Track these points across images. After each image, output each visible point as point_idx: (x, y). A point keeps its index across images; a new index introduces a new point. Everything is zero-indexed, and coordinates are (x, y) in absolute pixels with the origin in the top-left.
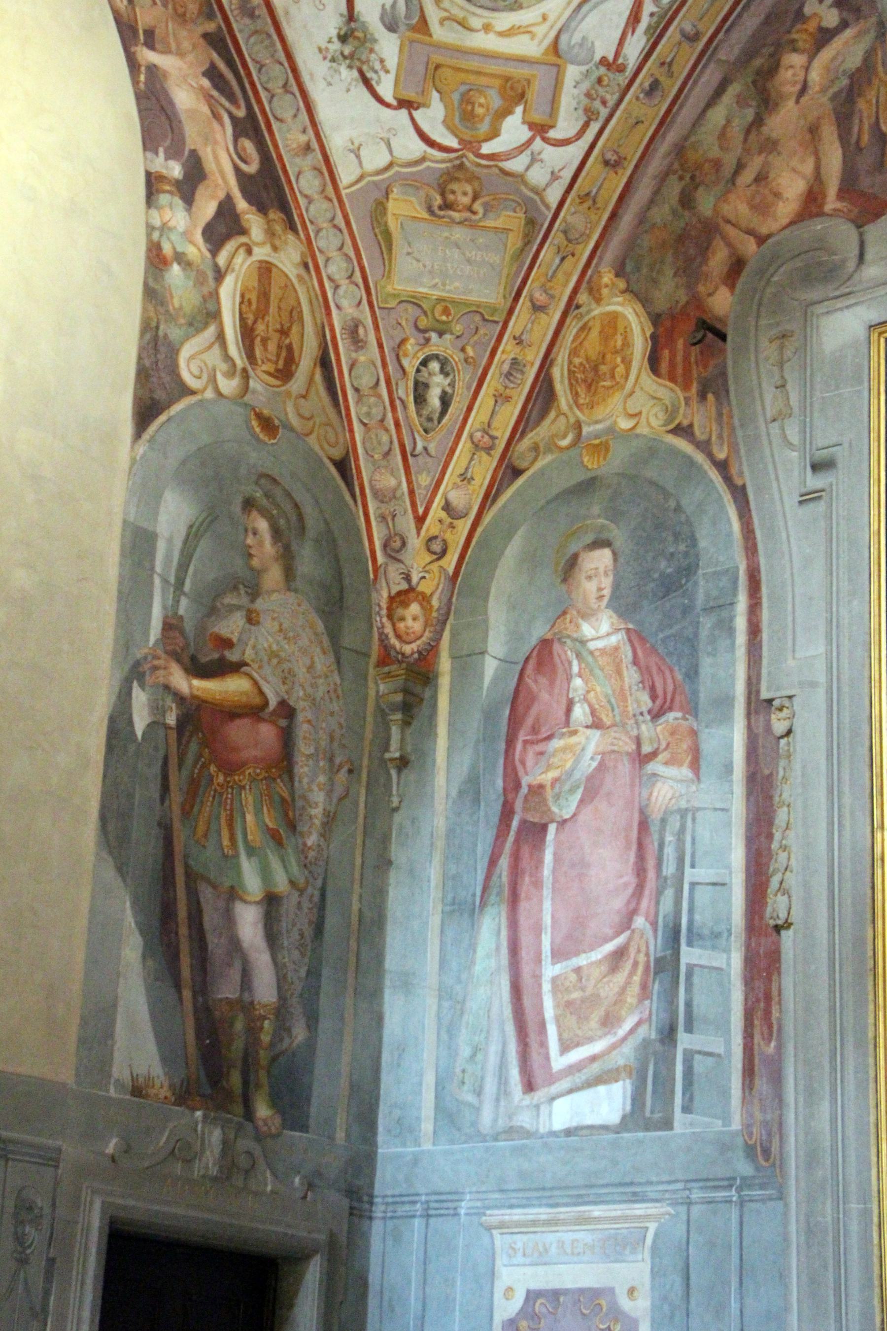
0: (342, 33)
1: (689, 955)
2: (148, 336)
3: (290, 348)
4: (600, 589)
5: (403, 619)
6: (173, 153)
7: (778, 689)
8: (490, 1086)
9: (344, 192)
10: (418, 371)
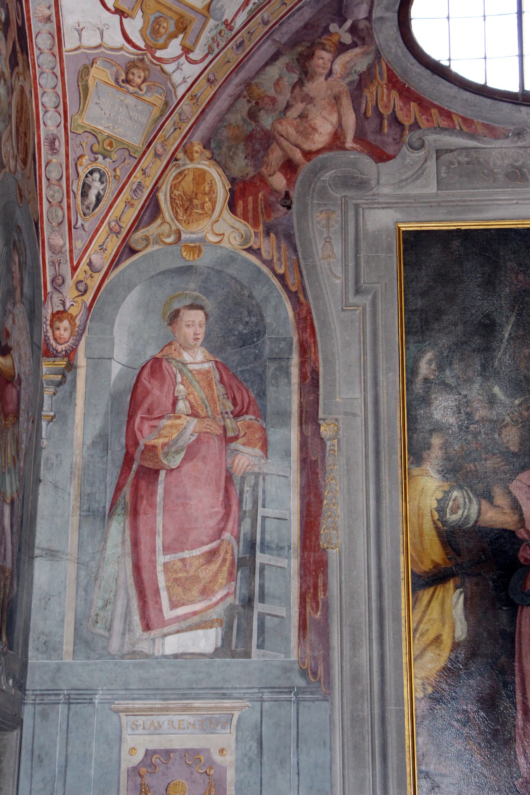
1: (261, 558)
4: (195, 334)
5: (58, 329)
7: (330, 414)
8: (118, 626)
9: (64, 54)
10: (87, 176)
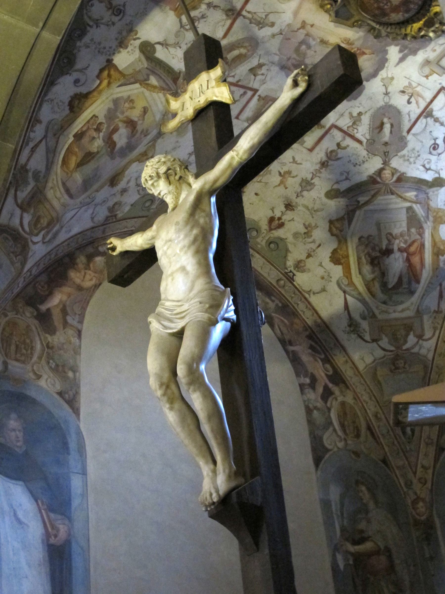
0: (349, 324)
2: (312, 436)
3: (357, 427)
6: (306, 376)
9: (362, 373)
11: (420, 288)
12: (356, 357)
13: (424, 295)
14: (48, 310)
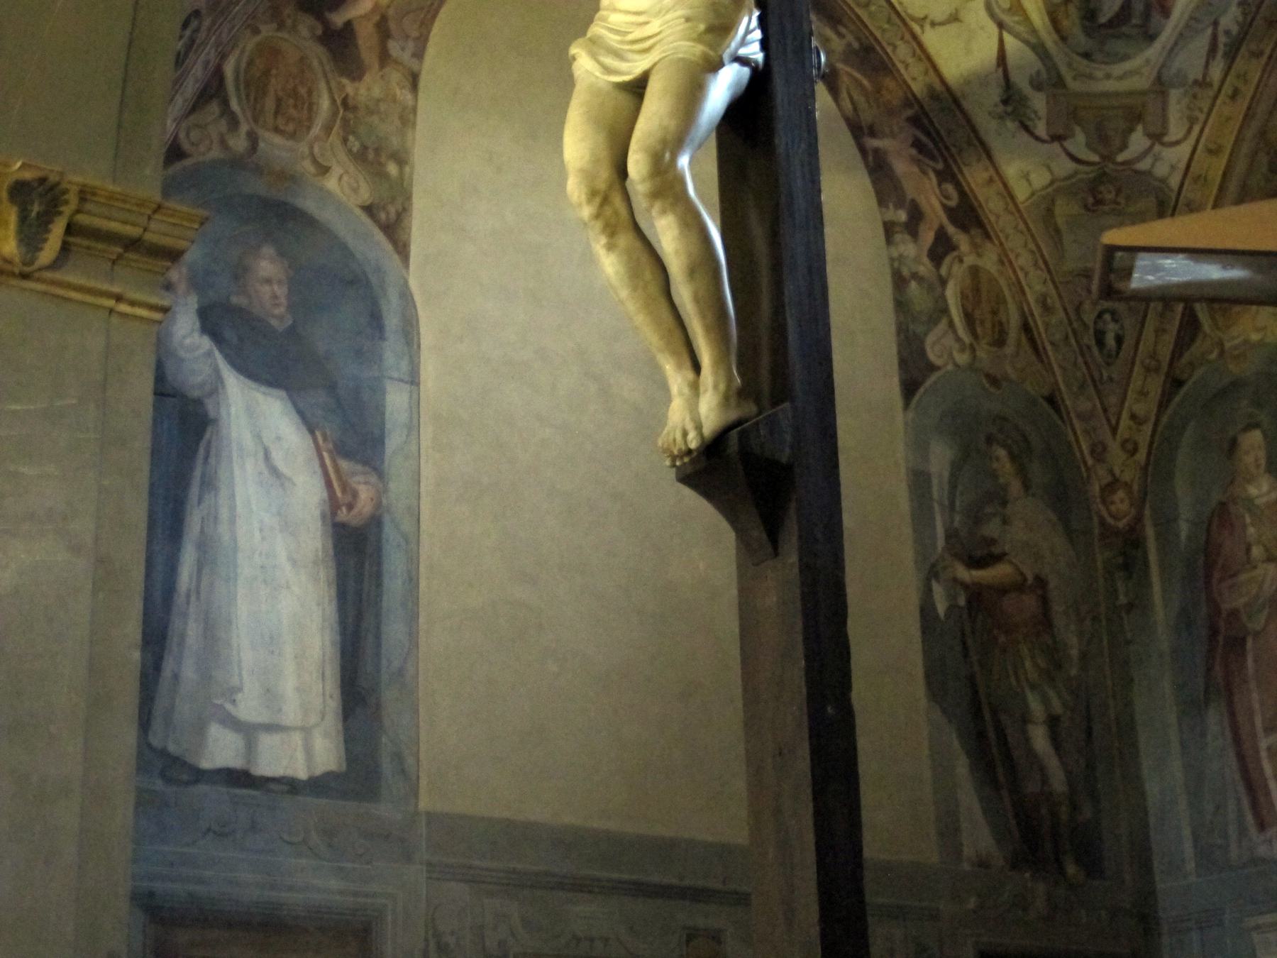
0: (1004, 98)
2: (902, 336)
3: (1001, 324)
4: (1256, 460)
5: (1113, 503)
6: (899, 204)
8: (1232, 830)
9: (1021, 206)
10: (1095, 323)
11: (1168, 31)
12: (1011, 170)
13: (1176, 44)
14: (349, 24)
